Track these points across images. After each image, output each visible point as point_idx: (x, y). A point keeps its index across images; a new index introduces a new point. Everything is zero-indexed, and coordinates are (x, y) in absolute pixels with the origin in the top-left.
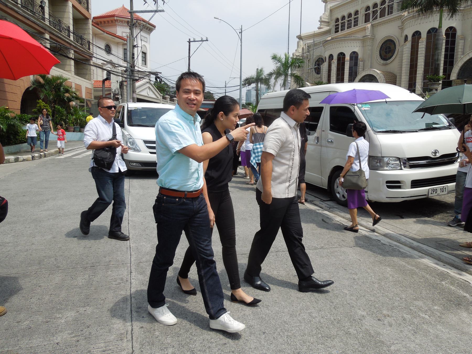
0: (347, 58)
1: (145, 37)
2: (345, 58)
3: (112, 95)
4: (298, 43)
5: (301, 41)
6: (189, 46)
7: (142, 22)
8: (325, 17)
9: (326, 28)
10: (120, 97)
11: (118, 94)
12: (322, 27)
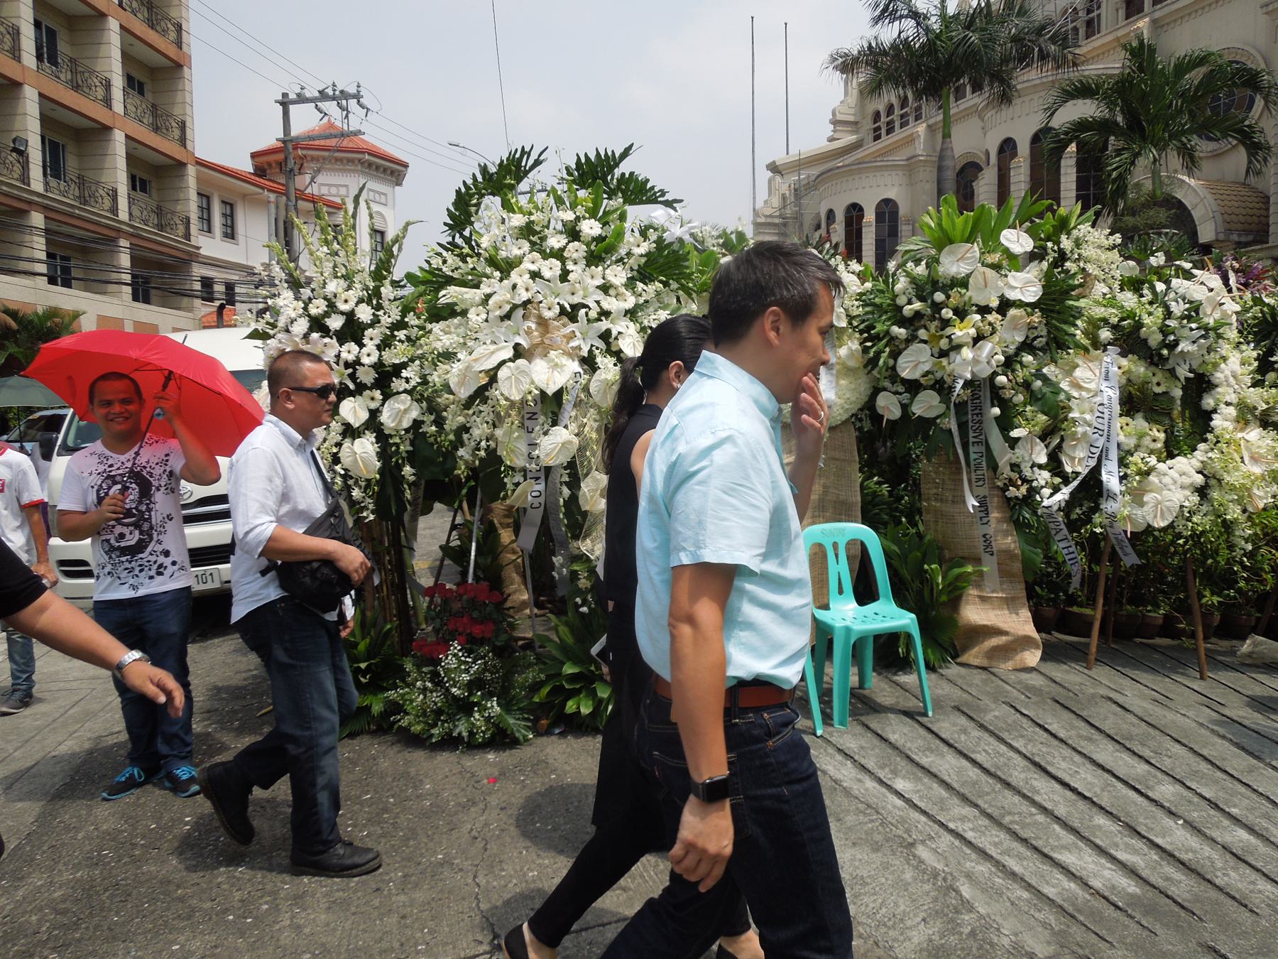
0: (870, 217)
1: (380, 193)
4: (770, 181)
5: (778, 178)
7: (367, 157)
8: (845, 109)
9: (850, 139)
12: (836, 136)
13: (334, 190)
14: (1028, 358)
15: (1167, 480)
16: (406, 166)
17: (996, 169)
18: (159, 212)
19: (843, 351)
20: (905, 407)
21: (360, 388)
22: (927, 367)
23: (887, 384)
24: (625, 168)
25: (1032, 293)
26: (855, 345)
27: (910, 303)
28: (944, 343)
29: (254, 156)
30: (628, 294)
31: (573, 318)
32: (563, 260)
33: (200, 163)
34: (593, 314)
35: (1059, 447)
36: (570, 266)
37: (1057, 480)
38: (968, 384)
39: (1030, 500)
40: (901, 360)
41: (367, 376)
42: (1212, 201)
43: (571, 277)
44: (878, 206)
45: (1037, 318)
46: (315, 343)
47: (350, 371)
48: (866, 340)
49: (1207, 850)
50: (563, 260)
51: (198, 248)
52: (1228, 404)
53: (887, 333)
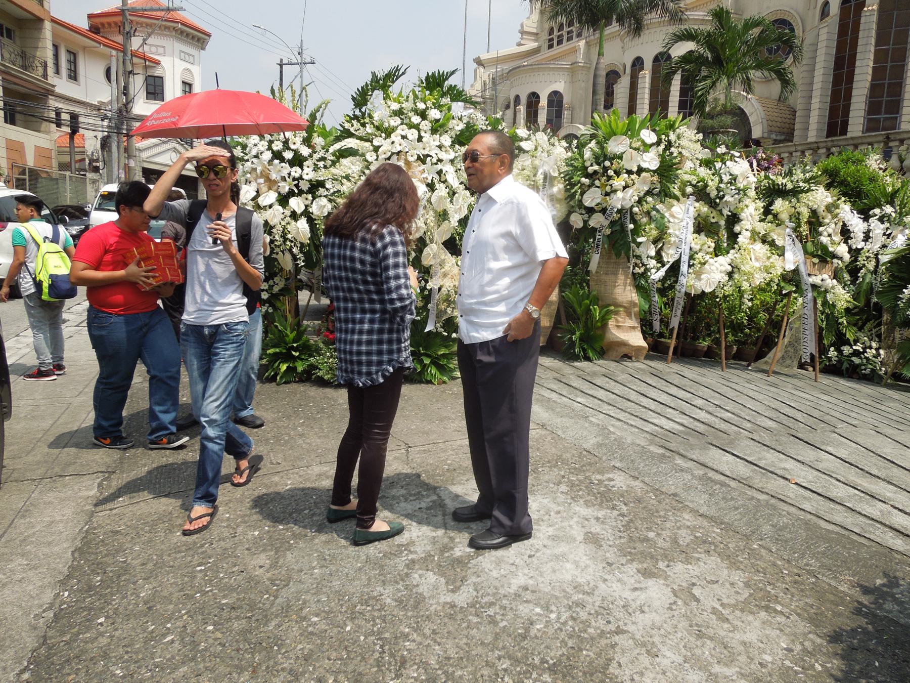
0: (544, 102)
1: (189, 55)
2: (539, 102)
3: (87, 161)
4: (475, 71)
5: (481, 69)
6: (281, 72)
9: (531, 45)
10: (100, 164)
11: (97, 160)
12: (523, 42)
13: (154, 49)
14: (650, 199)
15: (713, 268)
16: (209, 35)
17: (629, 78)
18: (23, 55)
19: (555, 189)
20: (585, 222)
21: (301, 193)
22: (598, 201)
23: (577, 209)
24: (451, 81)
25: (654, 165)
26: (561, 186)
27: (592, 165)
28: (608, 189)
29: (90, 16)
30: (451, 151)
31: (424, 162)
32: (419, 130)
33: (54, 21)
34: (434, 160)
35: (662, 247)
36: (423, 134)
37: (659, 265)
38: (619, 211)
39: (644, 275)
40: (585, 196)
41: (304, 186)
42: (762, 112)
43: (424, 140)
44: (550, 96)
45: (656, 178)
46: (276, 165)
47: (296, 182)
48: (567, 185)
49: (713, 418)
50: (419, 130)
51: (54, 86)
52: (747, 230)
53: (579, 182)
